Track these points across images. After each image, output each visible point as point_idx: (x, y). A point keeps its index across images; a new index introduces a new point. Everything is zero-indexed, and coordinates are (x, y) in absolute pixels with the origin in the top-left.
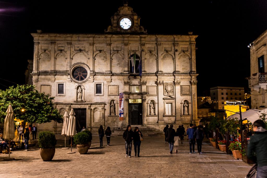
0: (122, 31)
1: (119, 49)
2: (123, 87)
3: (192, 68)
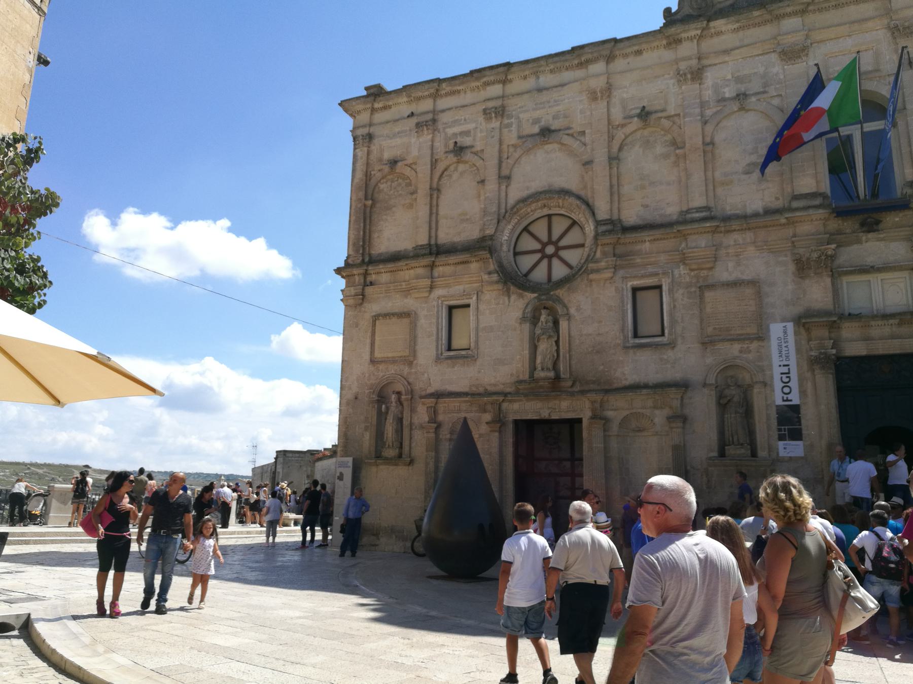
1: (755, 86)
2: (790, 287)
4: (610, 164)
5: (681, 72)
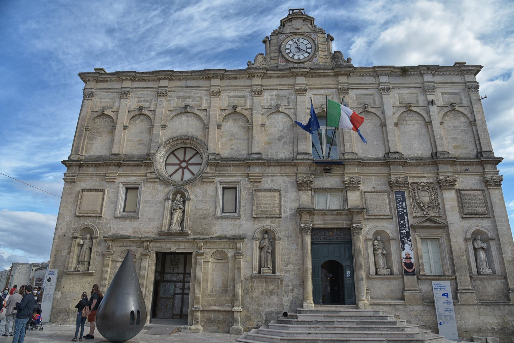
0: (291, 65)
3: (480, 143)
4: (218, 127)
5: (254, 90)
